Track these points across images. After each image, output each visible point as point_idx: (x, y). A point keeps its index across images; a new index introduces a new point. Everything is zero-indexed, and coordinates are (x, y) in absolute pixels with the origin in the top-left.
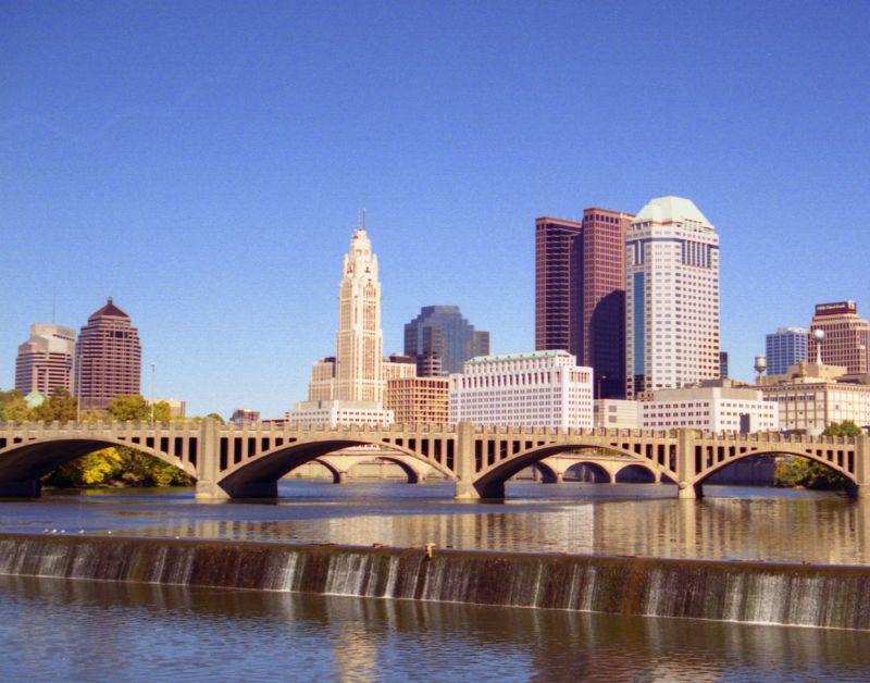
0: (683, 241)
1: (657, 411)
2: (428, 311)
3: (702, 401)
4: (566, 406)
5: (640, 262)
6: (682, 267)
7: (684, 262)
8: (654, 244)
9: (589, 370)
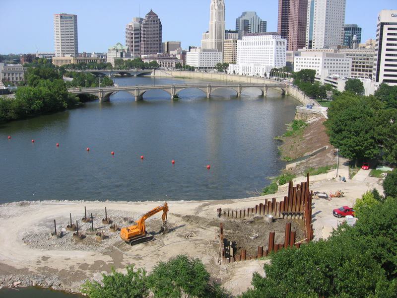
1: (301, 61)
2: (244, 14)
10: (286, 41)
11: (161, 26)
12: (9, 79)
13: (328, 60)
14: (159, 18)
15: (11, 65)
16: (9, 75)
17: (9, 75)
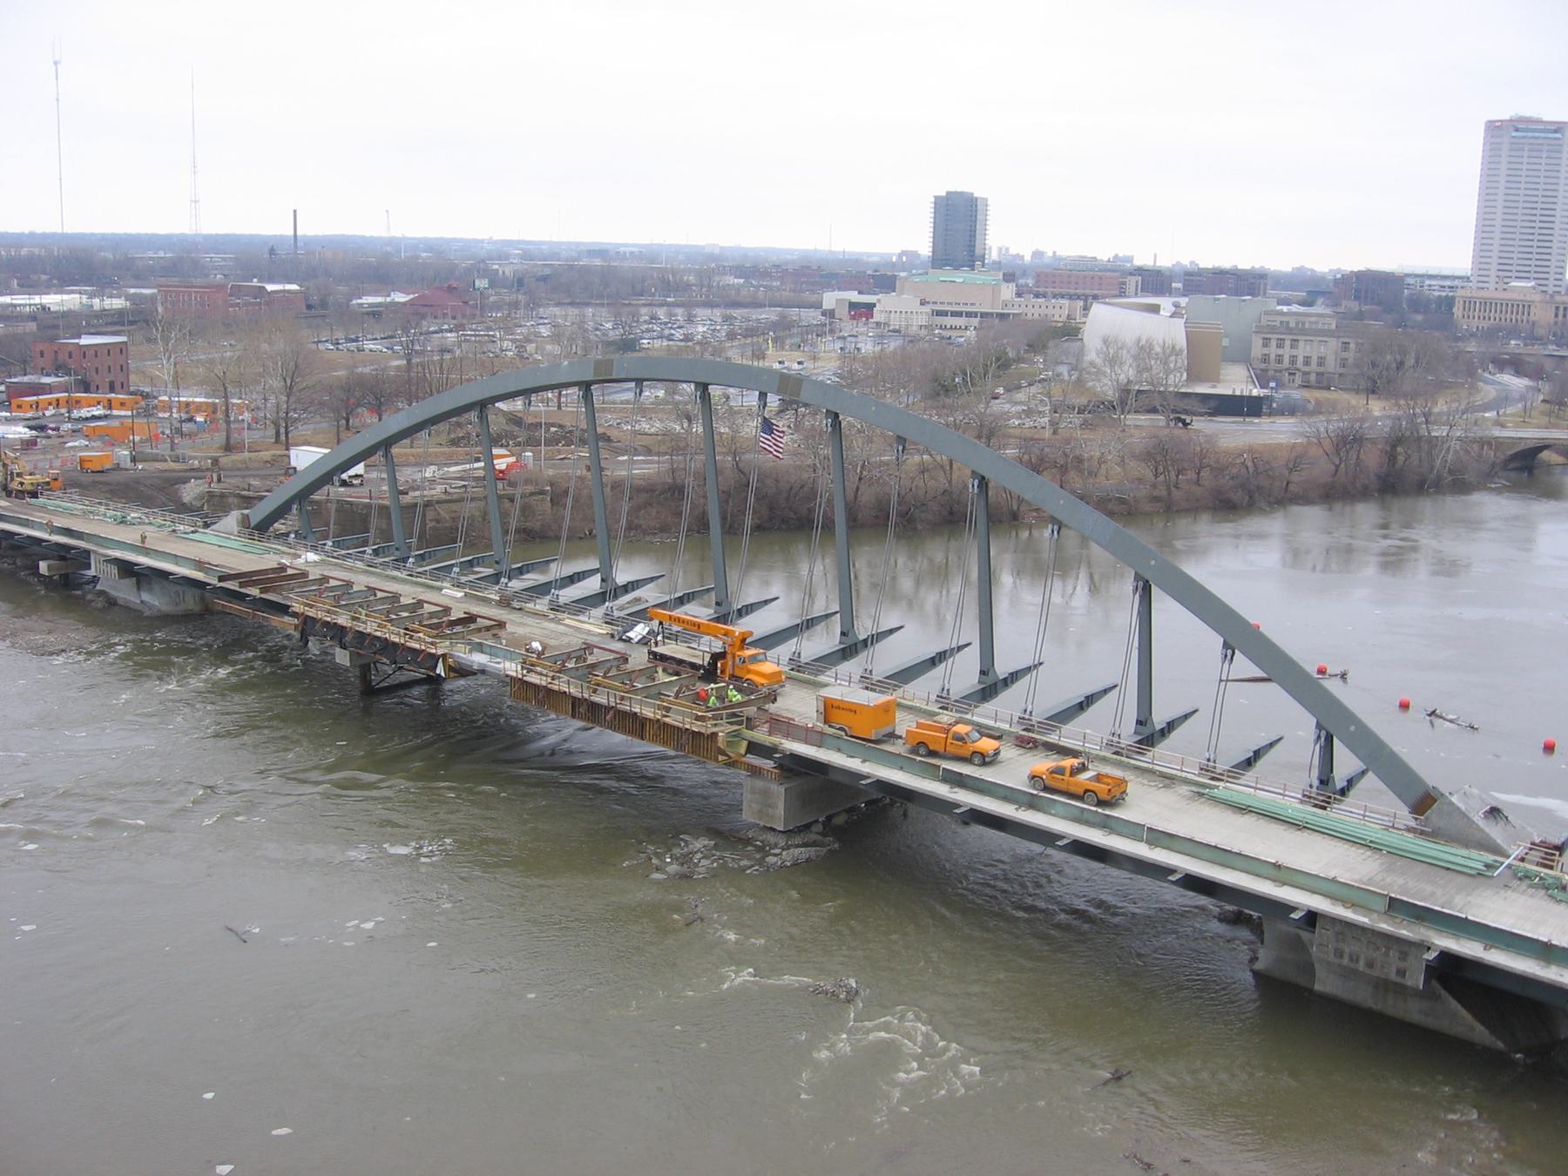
12: (1279, 359)
15: (1295, 308)
16: (1280, 345)
17: (1280, 345)
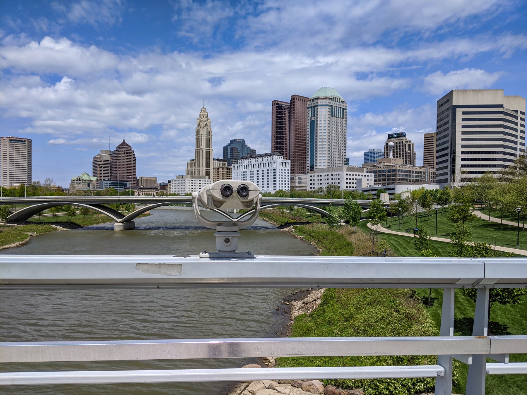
0: (332, 106)
1: (316, 178)
3: (337, 173)
4: (278, 177)
5: (313, 116)
6: (331, 117)
7: (332, 116)
8: (319, 107)
9: (289, 161)
10: (289, 161)
11: (135, 159)
13: (350, 175)
14: (132, 149)
